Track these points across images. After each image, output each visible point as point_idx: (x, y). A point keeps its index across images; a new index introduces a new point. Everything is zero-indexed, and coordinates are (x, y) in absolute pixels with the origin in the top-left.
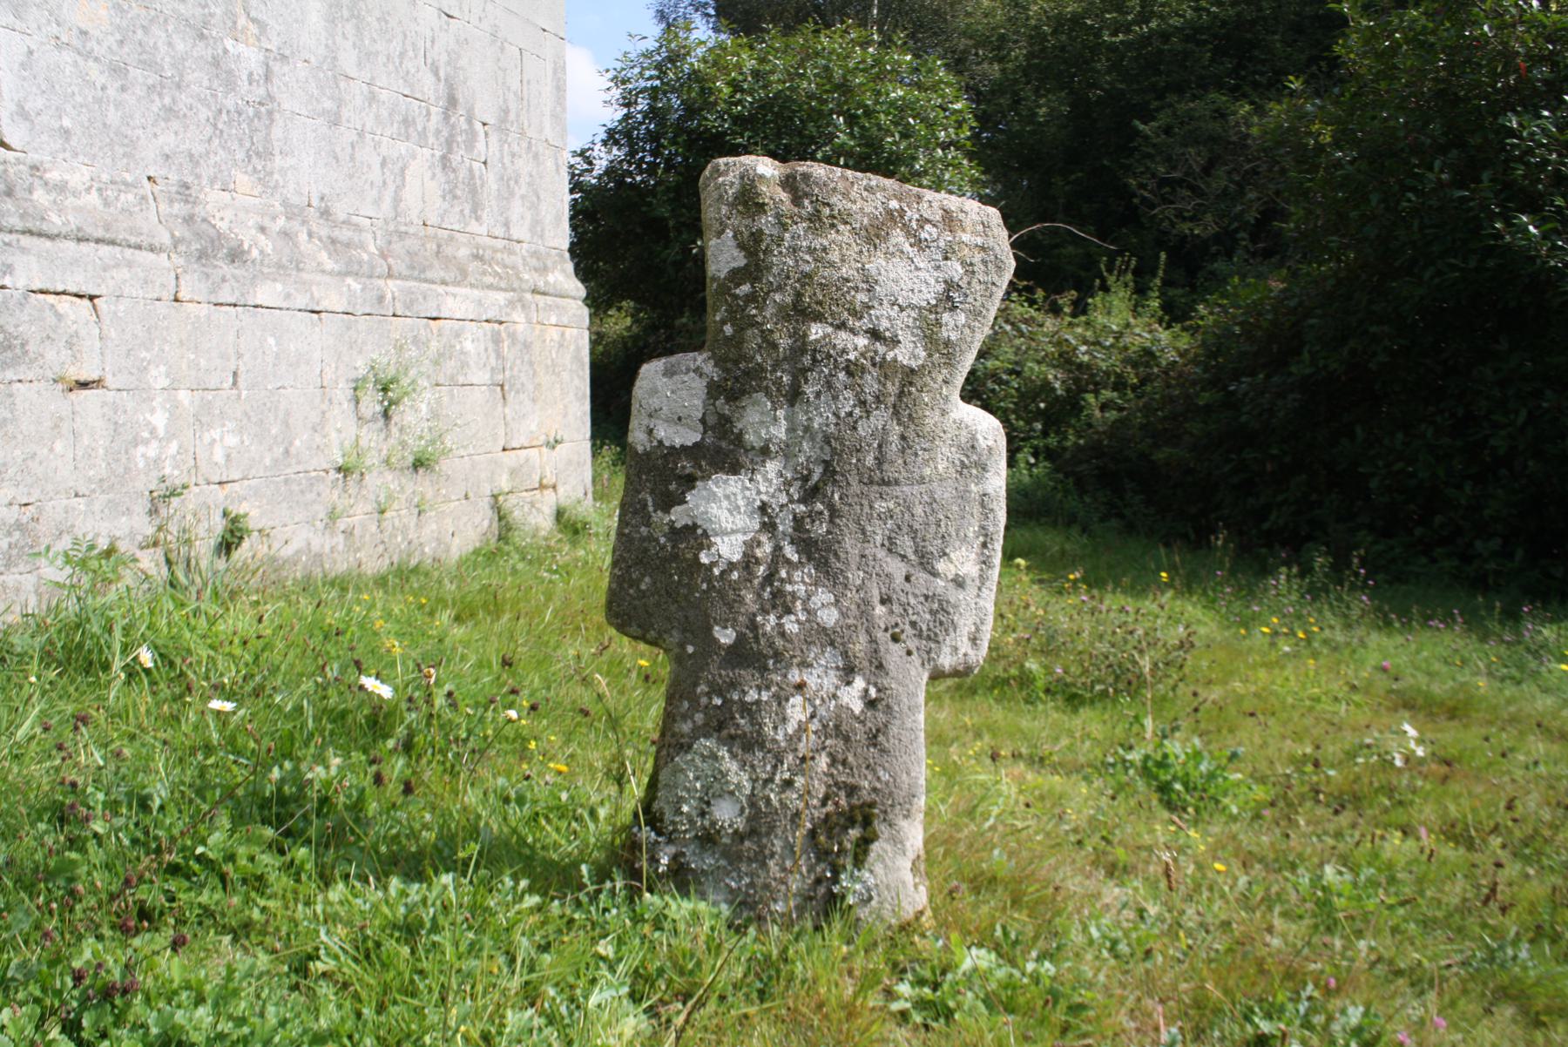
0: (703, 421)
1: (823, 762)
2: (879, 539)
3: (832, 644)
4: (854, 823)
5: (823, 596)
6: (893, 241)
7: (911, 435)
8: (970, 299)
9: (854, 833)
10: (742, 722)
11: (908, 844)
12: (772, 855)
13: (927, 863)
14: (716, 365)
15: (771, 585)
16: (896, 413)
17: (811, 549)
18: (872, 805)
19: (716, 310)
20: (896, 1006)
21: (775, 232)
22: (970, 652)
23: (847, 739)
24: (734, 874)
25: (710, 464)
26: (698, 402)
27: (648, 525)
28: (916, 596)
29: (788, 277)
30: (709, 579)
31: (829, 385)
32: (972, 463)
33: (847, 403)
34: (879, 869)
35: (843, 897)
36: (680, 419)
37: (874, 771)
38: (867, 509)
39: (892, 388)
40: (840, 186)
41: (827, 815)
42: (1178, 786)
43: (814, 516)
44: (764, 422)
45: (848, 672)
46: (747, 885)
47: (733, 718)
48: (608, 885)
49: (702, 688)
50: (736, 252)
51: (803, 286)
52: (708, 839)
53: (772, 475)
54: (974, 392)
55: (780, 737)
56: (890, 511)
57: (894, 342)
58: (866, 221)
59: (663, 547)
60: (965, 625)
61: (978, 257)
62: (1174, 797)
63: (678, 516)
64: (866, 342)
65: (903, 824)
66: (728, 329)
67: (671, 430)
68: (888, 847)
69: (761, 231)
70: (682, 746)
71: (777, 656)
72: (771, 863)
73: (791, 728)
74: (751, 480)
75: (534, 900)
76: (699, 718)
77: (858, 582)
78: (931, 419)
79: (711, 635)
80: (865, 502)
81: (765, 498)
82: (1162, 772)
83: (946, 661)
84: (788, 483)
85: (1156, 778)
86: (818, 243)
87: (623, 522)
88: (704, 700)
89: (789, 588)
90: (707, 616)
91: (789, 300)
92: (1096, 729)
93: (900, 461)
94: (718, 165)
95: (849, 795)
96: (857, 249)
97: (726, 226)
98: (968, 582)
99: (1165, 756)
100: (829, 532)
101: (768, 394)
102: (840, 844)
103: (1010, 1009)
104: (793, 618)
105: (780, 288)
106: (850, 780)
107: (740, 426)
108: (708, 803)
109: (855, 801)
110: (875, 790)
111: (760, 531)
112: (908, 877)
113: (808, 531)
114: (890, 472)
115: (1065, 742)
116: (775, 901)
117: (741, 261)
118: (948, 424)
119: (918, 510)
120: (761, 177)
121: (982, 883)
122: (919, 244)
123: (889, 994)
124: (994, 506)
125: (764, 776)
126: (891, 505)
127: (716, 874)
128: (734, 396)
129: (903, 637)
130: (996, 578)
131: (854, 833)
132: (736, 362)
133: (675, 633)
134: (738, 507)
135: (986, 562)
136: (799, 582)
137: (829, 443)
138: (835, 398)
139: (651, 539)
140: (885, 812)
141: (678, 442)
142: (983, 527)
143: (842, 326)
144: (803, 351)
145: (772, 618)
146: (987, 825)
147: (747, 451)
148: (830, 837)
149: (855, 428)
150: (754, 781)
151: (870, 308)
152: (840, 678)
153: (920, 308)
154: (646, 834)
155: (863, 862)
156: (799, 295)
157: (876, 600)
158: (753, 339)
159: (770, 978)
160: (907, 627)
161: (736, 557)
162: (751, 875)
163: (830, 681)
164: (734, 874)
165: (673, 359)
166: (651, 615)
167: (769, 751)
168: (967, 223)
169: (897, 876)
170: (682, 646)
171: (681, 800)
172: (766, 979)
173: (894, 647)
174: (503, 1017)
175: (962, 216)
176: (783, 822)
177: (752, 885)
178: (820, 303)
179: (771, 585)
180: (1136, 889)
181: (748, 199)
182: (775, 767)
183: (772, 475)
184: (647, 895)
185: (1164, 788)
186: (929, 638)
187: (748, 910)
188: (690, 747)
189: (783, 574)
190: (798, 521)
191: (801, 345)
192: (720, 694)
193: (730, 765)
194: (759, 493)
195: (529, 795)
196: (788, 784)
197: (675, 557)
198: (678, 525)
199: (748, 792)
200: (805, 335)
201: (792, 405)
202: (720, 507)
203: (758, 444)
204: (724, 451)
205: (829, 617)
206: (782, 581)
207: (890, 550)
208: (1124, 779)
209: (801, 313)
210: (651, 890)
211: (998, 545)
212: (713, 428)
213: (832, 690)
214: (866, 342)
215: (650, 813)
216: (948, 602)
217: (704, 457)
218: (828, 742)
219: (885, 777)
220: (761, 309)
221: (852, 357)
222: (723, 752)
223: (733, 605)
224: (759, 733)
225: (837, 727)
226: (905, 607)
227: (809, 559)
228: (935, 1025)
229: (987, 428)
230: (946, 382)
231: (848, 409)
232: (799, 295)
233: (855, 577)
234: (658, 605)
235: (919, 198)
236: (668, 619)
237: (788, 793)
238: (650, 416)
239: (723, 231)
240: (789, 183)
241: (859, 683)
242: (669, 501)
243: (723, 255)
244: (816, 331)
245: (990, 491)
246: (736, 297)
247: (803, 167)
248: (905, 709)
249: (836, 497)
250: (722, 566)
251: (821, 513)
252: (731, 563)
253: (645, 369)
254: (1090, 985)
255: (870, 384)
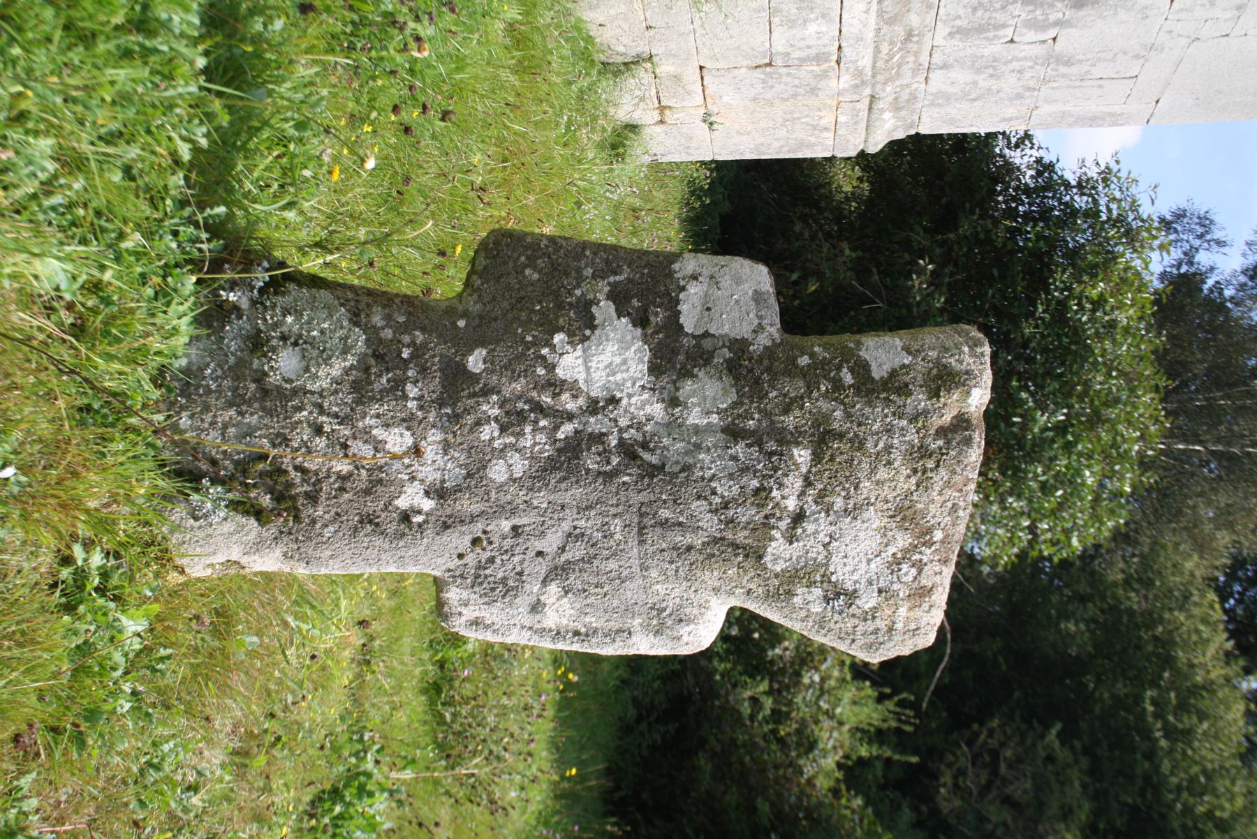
0: (706, 334)
1: (343, 467)
2: (582, 523)
3: (469, 475)
4: (276, 498)
5: (520, 466)
6: (899, 535)
7: (693, 556)
8: (836, 617)
9: (266, 501)
10: (384, 381)
11: (256, 557)
12: (241, 414)
13: (234, 580)
14: (766, 348)
15: (531, 410)
16: (716, 541)
17: (571, 450)
18: (297, 519)
19: (825, 347)
20: (78, 551)
21: (909, 410)
22: (464, 619)
23: (367, 492)
24: (219, 372)
25: (660, 343)
26: (726, 329)
27: (594, 276)
28: (522, 562)
29: (859, 425)
30: (536, 343)
31: (744, 470)
32: (663, 619)
33: (726, 489)
34: (228, 527)
35: (197, 490)
36: (708, 309)
37: (333, 521)
38: (613, 511)
39: (742, 536)
40: (958, 478)
41: (286, 472)
42: (338, 809)
43: (605, 454)
44: (706, 401)
45: (439, 492)
46: (208, 386)
47: (388, 371)
48: (204, 236)
49: (420, 337)
50: (887, 368)
51: (851, 441)
52: (257, 343)
53: (648, 409)
54: (740, 620)
55: (368, 421)
56: (612, 535)
57: (791, 539)
58: (920, 506)
59: (570, 293)
60: (492, 614)
61: (881, 624)
62: (327, 805)
63: (604, 309)
64: (791, 508)
65: (278, 552)
66: (804, 361)
67: (696, 300)
68: (252, 537)
69: (910, 394)
70: (357, 315)
71: (456, 418)
72: (232, 412)
73: (378, 433)
74: (643, 387)
75: (185, 152)
76: (388, 334)
77: (535, 503)
78: (710, 578)
79: (477, 347)
80: (620, 509)
81: (624, 402)
82: (354, 791)
83: (453, 595)
84: (640, 427)
85: (345, 786)
86: (896, 455)
87: (598, 247)
88: (406, 339)
89: (528, 429)
90: (497, 342)
91: (836, 425)
92: (401, 717)
93: (664, 545)
94: (982, 345)
95: (307, 495)
96: (890, 497)
97: (915, 357)
98: (538, 617)
99: (371, 795)
100: (588, 471)
101: (734, 405)
102: (255, 485)
103: (79, 671)
104: (496, 434)
105: (848, 416)
106: (323, 495)
107: (701, 375)
108: (296, 344)
109: (301, 501)
110: (314, 522)
111: (589, 397)
112: (220, 558)
113: (589, 449)
114: (652, 535)
115: (387, 684)
116: (192, 417)
117: (877, 373)
118: (704, 595)
119: (612, 565)
120: (968, 393)
121: (223, 622)
122: (896, 562)
123: (88, 545)
124: (618, 643)
125: (326, 405)
126: (618, 536)
127: (218, 353)
128: (732, 367)
129: (478, 550)
130: (543, 644)
131: (266, 501)
132: (769, 370)
133: (479, 306)
134: (614, 374)
135: (558, 634)
136: (534, 440)
137: (683, 470)
138: (731, 476)
139: (580, 279)
140: (290, 533)
141: (683, 308)
142: (595, 631)
143: (808, 483)
144: (780, 442)
145: (496, 411)
146: (290, 619)
147: (674, 382)
148: (261, 474)
149: (699, 498)
150: (321, 394)
151: (827, 512)
152: (433, 484)
153: (827, 565)
154: (260, 277)
155: (235, 510)
156: (841, 436)
157: (517, 521)
158: (795, 387)
159: (105, 416)
160: (488, 554)
161: (560, 372)
162: (219, 391)
163: (429, 473)
164: (219, 372)
165: (773, 301)
166: (498, 280)
167: (352, 409)
168: (918, 613)
169: (220, 546)
170: (465, 315)
171: (298, 314)
172: (103, 412)
173: (467, 540)
174: (47, 134)
175: (925, 606)
176: (276, 425)
177: (209, 391)
178: (832, 459)
179: (531, 410)
180: (221, 780)
181: (944, 380)
182: (336, 416)
183: (648, 409)
184: (194, 279)
185: (335, 794)
186: (477, 576)
187: (181, 387)
188: (356, 324)
189: (543, 423)
190: (600, 438)
191: (787, 439)
192: (413, 356)
193: (337, 368)
194: (630, 396)
195: (308, 133)
196: (318, 430)
197: (560, 306)
198: (594, 309)
199: (309, 387)
200: (798, 444)
201: (723, 431)
202: (614, 355)
203: (681, 395)
204: (673, 357)
205: (498, 472)
206: (536, 422)
207: (570, 535)
208: (346, 753)
209: (822, 438)
210: (199, 282)
211: (576, 647)
212: (698, 345)
213: (420, 476)
214: (791, 508)
215: (284, 280)
216: (516, 596)
217: (667, 337)
218: (364, 472)
219: (327, 532)
220: (826, 395)
221: (775, 493)
222: (351, 360)
223: (510, 369)
224: (372, 399)
225: (380, 481)
226: (510, 552)
227: (559, 451)
228: (58, 593)
229: (701, 635)
230: (749, 592)
231: (719, 490)
232: (841, 436)
233: (541, 499)
234: (509, 288)
235: (945, 562)
236: (494, 299)
237: (308, 430)
238: (712, 277)
239: (910, 353)
240: (962, 422)
241: (428, 505)
242: (619, 298)
243: (883, 352)
244: (802, 455)
245: (634, 639)
246: (839, 368)
247: (979, 438)
248: (400, 553)
249: (626, 479)
250: (551, 358)
251: (608, 463)
252: (554, 366)
253: (763, 269)
254: (109, 747)
255: (747, 514)
